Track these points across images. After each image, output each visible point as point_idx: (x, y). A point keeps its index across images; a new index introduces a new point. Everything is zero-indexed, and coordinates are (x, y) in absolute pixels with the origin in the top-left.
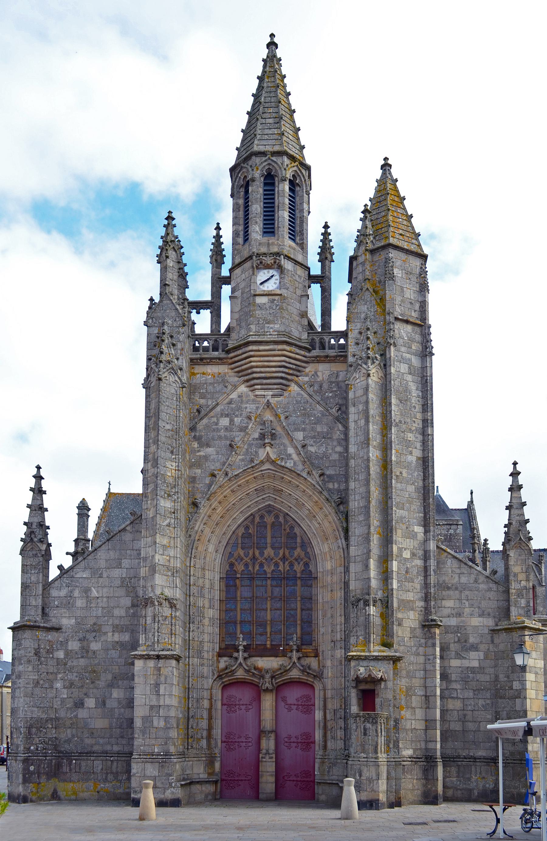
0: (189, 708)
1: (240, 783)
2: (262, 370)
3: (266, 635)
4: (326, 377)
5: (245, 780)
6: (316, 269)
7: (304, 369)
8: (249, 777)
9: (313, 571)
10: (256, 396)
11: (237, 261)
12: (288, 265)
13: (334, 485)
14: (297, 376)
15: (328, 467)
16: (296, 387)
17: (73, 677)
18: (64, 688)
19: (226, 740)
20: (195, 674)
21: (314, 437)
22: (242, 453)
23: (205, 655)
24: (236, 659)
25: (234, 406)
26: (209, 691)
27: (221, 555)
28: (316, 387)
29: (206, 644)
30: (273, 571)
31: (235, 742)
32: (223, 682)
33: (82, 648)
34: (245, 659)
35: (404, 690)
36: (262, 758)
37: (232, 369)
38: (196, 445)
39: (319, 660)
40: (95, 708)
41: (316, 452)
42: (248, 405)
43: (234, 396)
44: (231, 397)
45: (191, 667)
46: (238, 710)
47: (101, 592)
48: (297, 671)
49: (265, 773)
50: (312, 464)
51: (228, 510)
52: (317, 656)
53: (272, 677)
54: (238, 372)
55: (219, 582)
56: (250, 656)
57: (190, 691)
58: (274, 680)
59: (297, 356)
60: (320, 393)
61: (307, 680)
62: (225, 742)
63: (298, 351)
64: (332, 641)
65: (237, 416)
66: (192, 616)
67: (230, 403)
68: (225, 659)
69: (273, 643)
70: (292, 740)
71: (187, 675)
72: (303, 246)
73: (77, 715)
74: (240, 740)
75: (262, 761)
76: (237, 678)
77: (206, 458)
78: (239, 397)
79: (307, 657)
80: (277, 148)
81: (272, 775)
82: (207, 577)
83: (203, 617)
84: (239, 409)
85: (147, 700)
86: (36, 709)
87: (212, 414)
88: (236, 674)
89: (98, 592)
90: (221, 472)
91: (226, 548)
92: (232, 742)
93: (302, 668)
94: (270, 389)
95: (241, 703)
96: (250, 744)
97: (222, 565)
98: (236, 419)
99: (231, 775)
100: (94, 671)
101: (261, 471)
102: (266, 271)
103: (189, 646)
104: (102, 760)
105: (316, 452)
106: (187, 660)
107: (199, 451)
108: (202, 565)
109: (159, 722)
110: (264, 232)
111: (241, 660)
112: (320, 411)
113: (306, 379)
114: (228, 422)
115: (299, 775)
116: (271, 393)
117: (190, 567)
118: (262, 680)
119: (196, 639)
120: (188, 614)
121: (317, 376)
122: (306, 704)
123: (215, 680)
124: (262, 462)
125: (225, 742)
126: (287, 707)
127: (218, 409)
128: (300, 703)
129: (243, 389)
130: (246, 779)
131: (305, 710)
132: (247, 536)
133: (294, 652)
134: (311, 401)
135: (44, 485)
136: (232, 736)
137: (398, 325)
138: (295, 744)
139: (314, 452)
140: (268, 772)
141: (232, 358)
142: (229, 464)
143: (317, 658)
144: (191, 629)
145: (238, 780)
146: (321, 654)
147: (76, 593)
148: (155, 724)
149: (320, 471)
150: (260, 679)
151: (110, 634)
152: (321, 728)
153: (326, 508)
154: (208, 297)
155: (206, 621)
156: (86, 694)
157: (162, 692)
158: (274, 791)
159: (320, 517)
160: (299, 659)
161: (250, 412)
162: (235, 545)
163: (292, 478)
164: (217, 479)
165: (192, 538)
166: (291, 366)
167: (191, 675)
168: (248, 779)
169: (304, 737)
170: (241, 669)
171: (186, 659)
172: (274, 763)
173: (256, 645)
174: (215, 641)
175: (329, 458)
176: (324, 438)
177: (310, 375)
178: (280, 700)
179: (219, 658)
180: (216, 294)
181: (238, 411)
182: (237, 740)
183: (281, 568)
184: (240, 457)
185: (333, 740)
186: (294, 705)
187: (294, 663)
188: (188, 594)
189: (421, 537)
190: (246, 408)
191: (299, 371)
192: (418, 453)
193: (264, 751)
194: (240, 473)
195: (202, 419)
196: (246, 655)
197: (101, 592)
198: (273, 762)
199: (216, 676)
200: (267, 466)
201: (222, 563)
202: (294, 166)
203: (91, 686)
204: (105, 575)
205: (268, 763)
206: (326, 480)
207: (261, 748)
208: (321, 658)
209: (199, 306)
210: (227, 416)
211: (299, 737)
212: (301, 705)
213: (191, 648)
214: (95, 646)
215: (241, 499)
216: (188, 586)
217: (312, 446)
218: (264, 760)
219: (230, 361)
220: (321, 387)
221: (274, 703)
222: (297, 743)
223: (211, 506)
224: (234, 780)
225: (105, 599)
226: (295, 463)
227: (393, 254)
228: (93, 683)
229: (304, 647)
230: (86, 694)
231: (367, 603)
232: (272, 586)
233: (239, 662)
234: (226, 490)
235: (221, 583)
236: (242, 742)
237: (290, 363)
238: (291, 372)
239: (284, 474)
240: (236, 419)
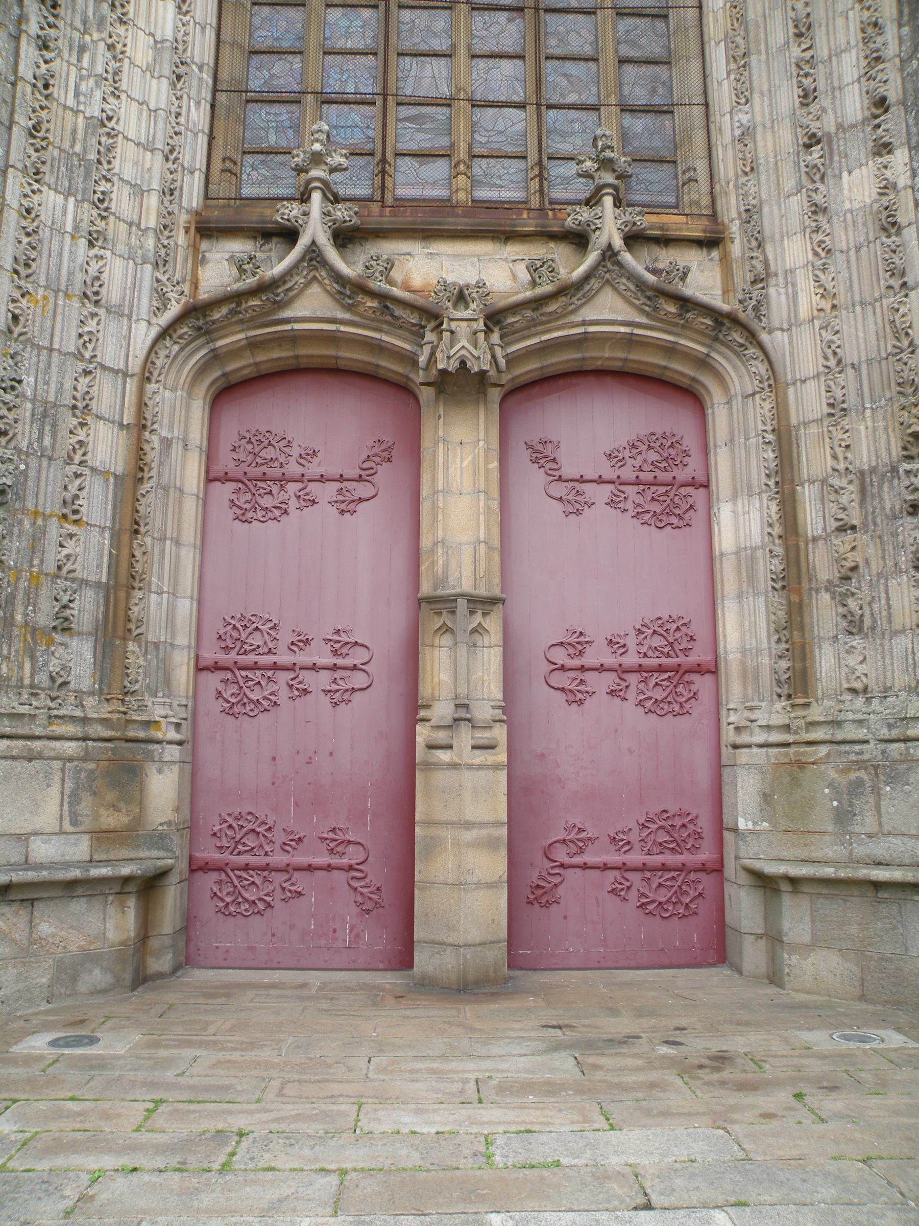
1: (301, 881)
5: (329, 868)
8: (353, 856)
19: (222, 657)
26: (131, 385)
31: (275, 667)
32: (215, 357)
36: (431, 747)
39: (725, 260)
46: (293, 504)
48: (619, 303)
49: (448, 834)
61: (670, 350)
62: (217, 667)
64: (812, 141)
68: (239, 247)
70: (591, 658)
74: (302, 658)
75: (429, 766)
76: (294, 339)
81: (490, 844)
88: (287, 313)
92: (255, 667)
93: (651, 278)
95: (314, 469)
96: (359, 679)
99: (251, 842)
115: (634, 837)
118: (430, 336)
122: (663, 476)
123: (165, 333)
125: (217, 667)
126: (559, 489)
128: (628, 473)
130: (336, 861)
131: (656, 507)
133: (608, 201)
136: (256, 640)
138: (610, 679)
140: (468, 825)
143: (715, 254)
145: (285, 869)
146: (735, 228)
150: (418, 334)
152: (764, 581)
158: (504, 934)
168: (344, 861)
169: (657, 641)
170: (315, 289)
172: (503, 776)
178: (521, 456)
179: (204, 245)
182: (284, 658)
185: (856, 641)
186: (600, 481)
187: (609, 253)
193: (442, 711)
198: (496, 767)
199: (174, 310)
205: (468, 777)
207: (425, 690)
208: (736, 249)
211: (631, 642)
212: (637, 482)
218: (444, 756)
221: (495, 464)
222: (622, 671)
224: (267, 868)
233: (303, 242)
236: (314, 668)
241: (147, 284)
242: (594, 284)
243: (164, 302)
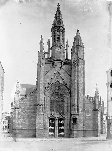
6: (66, 48)
11: (53, 45)
12: (61, 47)
72: (64, 44)
80: (60, 25)
137: (80, 60)
154: (47, 52)
159: (66, 91)
162: (51, 96)
180: (49, 51)
189: (83, 96)
192: (83, 82)
200: (57, 82)
209: (46, 53)
227: (79, 47)
231: (74, 106)
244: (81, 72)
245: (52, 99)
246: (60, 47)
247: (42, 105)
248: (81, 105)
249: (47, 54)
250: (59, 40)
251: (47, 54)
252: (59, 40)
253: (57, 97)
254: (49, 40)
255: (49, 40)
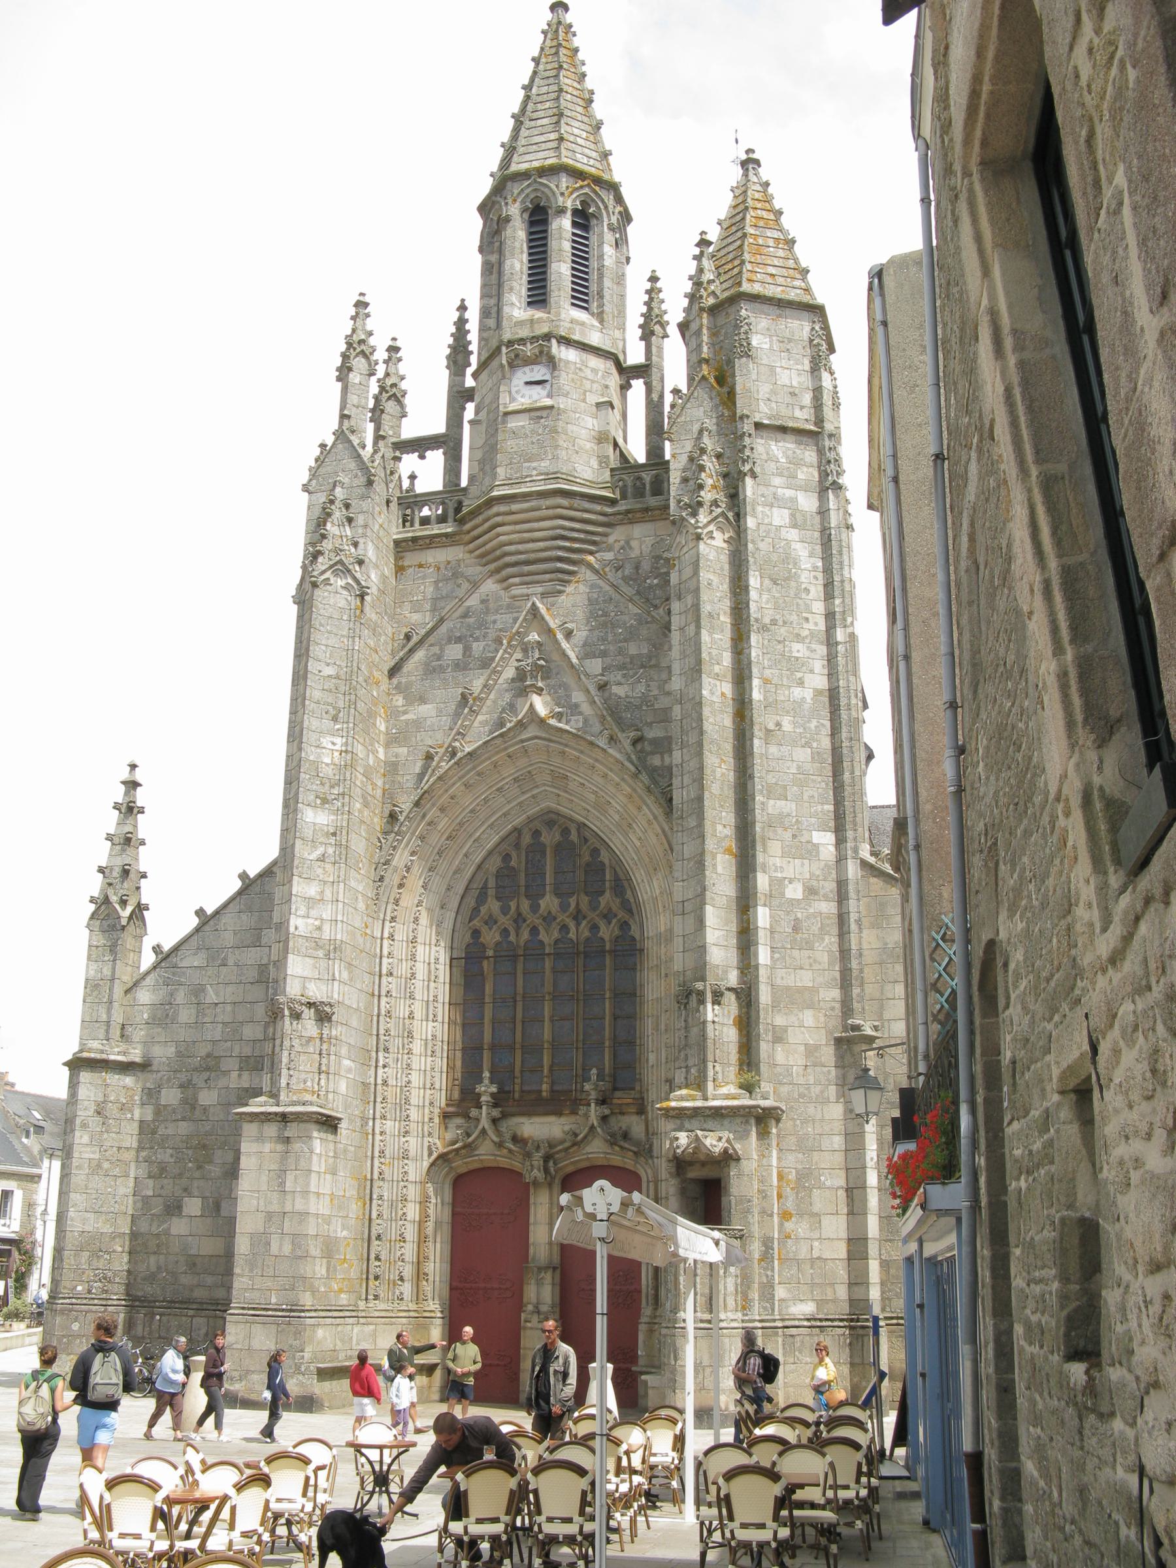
0: (370, 1219)
2: (520, 547)
3: (542, 1071)
4: (646, 549)
7: (604, 539)
9: (638, 938)
10: (513, 597)
13: (662, 760)
14: (591, 553)
15: (652, 723)
16: (589, 573)
17: (166, 1156)
18: (150, 1177)
20: (387, 1153)
21: (622, 667)
22: (484, 709)
23: (414, 1114)
24: (478, 1120)
25: (471, 620)
27: (453, 915)
28: (628, 571)
29: (414, 1092)
30: (556, 942)
33: (184, 1101)
34: (494, 1121)
35: (792, 1176)
36: (526, 1321)
37: (471, 552)
38: (399, 701)
40: (201, 1216)
41: (627, 697)
42: (498, 617)
43: (473, 601)
44: (467, 604)
45: (378, 1137)
47: (222, 994)
50: (619, 721)
51: (461, 824)
52: (641, 1111)
53: (547, 1158)
54: (482, 556)
55: (448, 967)
56: (505, 1116)
57: (376, 1185)
58: (551, 1163)
59: (586, 516)
60: (635, 580)
63: (587, 505)
65: (477, 640)
66: (382, 1038)
67: (465, 615)
69: (556, 1088)
71: (369, 1154)
73: (169, 1229)
75: (525, 1328)
77: (418, 724)
78: (483, 602)
79: (622, 1113)
82: (420, 956)
83: (410, 1035)
84: (482, 625)
85: (262, 1203)
86: (91, 1216)
87: (431, 639)
89: (217, 994)
90: (443, 750)
91: (465, 900)
94: (538, 582)
97: (456, 934)
98: (475, 645)
100: (204, 1147)
101: (522, 741)
102: (527, 369)
103: (375, 1097)
104: (207, 1317)
105: (627, 697)
106: (371, 1123)
107: (405, 713)
108: (411, 934)
109: (281, 1245)
110: (529, 303)
111: (485, 1122)
112: (636, 615)
113: (609, 556)
114: (461, 652)
116: (540, 590)
117: (382, 939)
119: (392, 1082)
120: (375, 1032)
121: (631, 548)
124: (521, 725)
127: (443, 629)
129: (490, 586)
132: (506, 874)
133: (593, 1105)
134: (618, 597)
135: (141, 797)
139: (623, 695)
141: (469, 532)
142: (459, 733)
144: (381, 1063)
147: (180, 997)
148: (274, 1249)
149: (632, 734)
151: (234, 1074)
153: (648, 806)
155: (417, 1047)
156: (185, 1190)
157: (289, 1186)
160: (604, 1119)
161: (501, 630)
162: (482, 898)
163: (582, 752)
164: (434, 763)
165: (387, 880)
166: (576, 535)
167: (377, 1154)
171: (367, 1123)
173: (522, 1091)
174: (437, 1086)
175: (653, 705)
176: (643, 666)
177: (617, 549)
181: (479, 628)
183: (572, 935)
184: (480, 718)
187: (592, 1127)
188: (376, 993)
190: (495, 622)
191: (594, 543)
193: (530, 1308)
194: (478, 748)
195: (412, 651)
196: (496, 1113)
197: (222, 994)
199: (435, 1155)
201: (457, 928)
202: (581, 187)
203: (197, 1174)
204: (231, 962)
206: (648, 748)
210: (459, 640)
213: (379, 1099)
214: (207, 1098)
215: (486, 800)
216: (377, 978)
217: (620, 684)
218: (529, 1325)
219: (467, 538)
220: (637, 568)
223: (424, 816)
225: (229, 1008)
226: (586, 721)
228: (199, 1168)
229: (618, 1094)
230: (185, 1190)
232: (554, 971)
233: (480, 1127)
234: (454, 784)
235: (454, 969)
237: (573, 530)
238: (577, 546)
239: (566, 745)
240: (475, 645)
241: (426, 1144)
242: (590, 1138)
243: (430, 1154)
244: (782, 578)
245: (490, 937)
246: (552, 363)
247: (308, 1013)
248: (805, 979)
249: (436, 458)
250: (539, 295)
251: (436, 458)
252: (539, 295)
253: (549, 902)
254: (461, 323)
255: (461, 323)
